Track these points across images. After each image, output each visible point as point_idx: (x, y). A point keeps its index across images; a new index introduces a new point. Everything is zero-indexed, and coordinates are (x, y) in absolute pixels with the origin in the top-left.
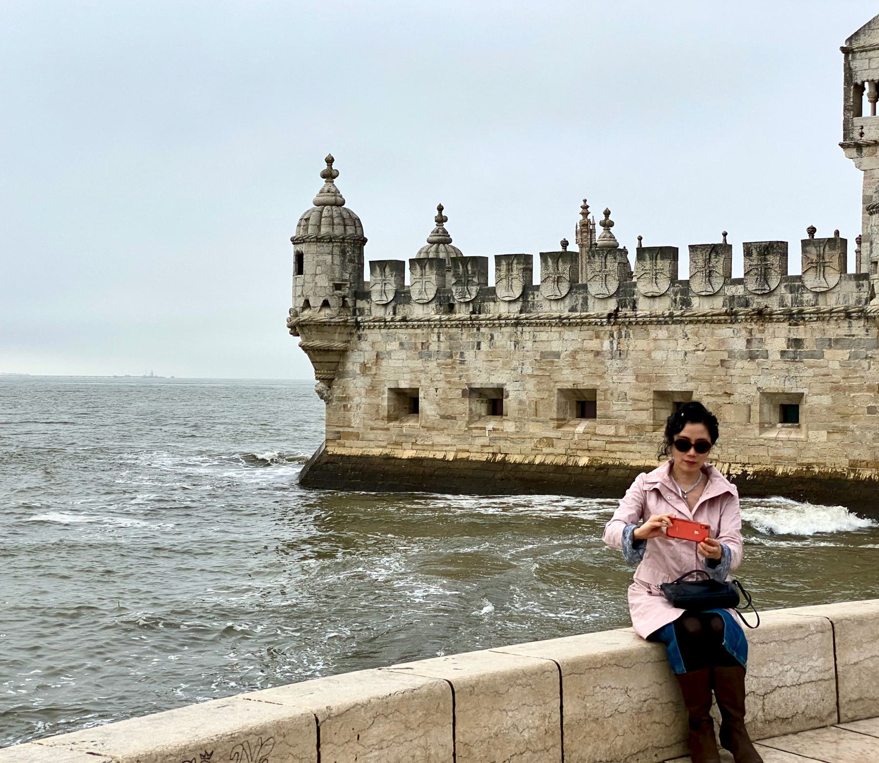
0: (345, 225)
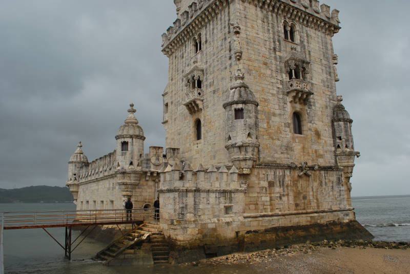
0: (77, 158)
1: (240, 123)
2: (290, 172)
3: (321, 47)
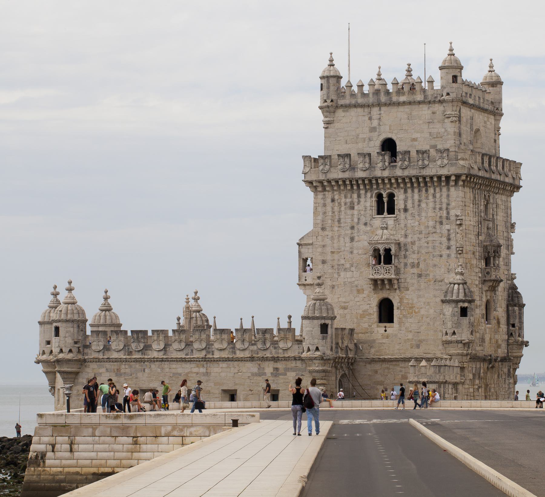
0: (79, 314)
1: (465, 321)
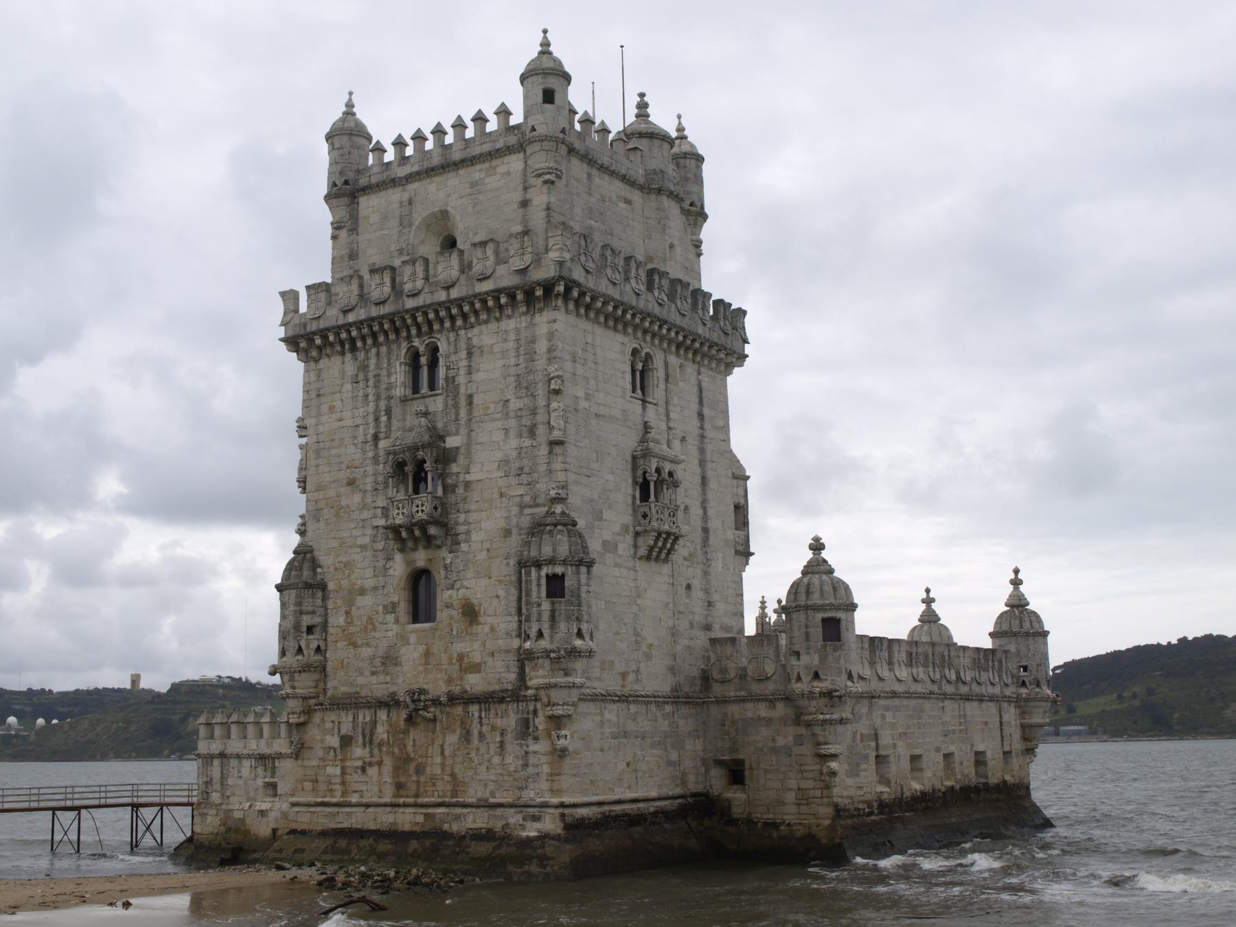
2: (389, 712)
3: (513, 361)
